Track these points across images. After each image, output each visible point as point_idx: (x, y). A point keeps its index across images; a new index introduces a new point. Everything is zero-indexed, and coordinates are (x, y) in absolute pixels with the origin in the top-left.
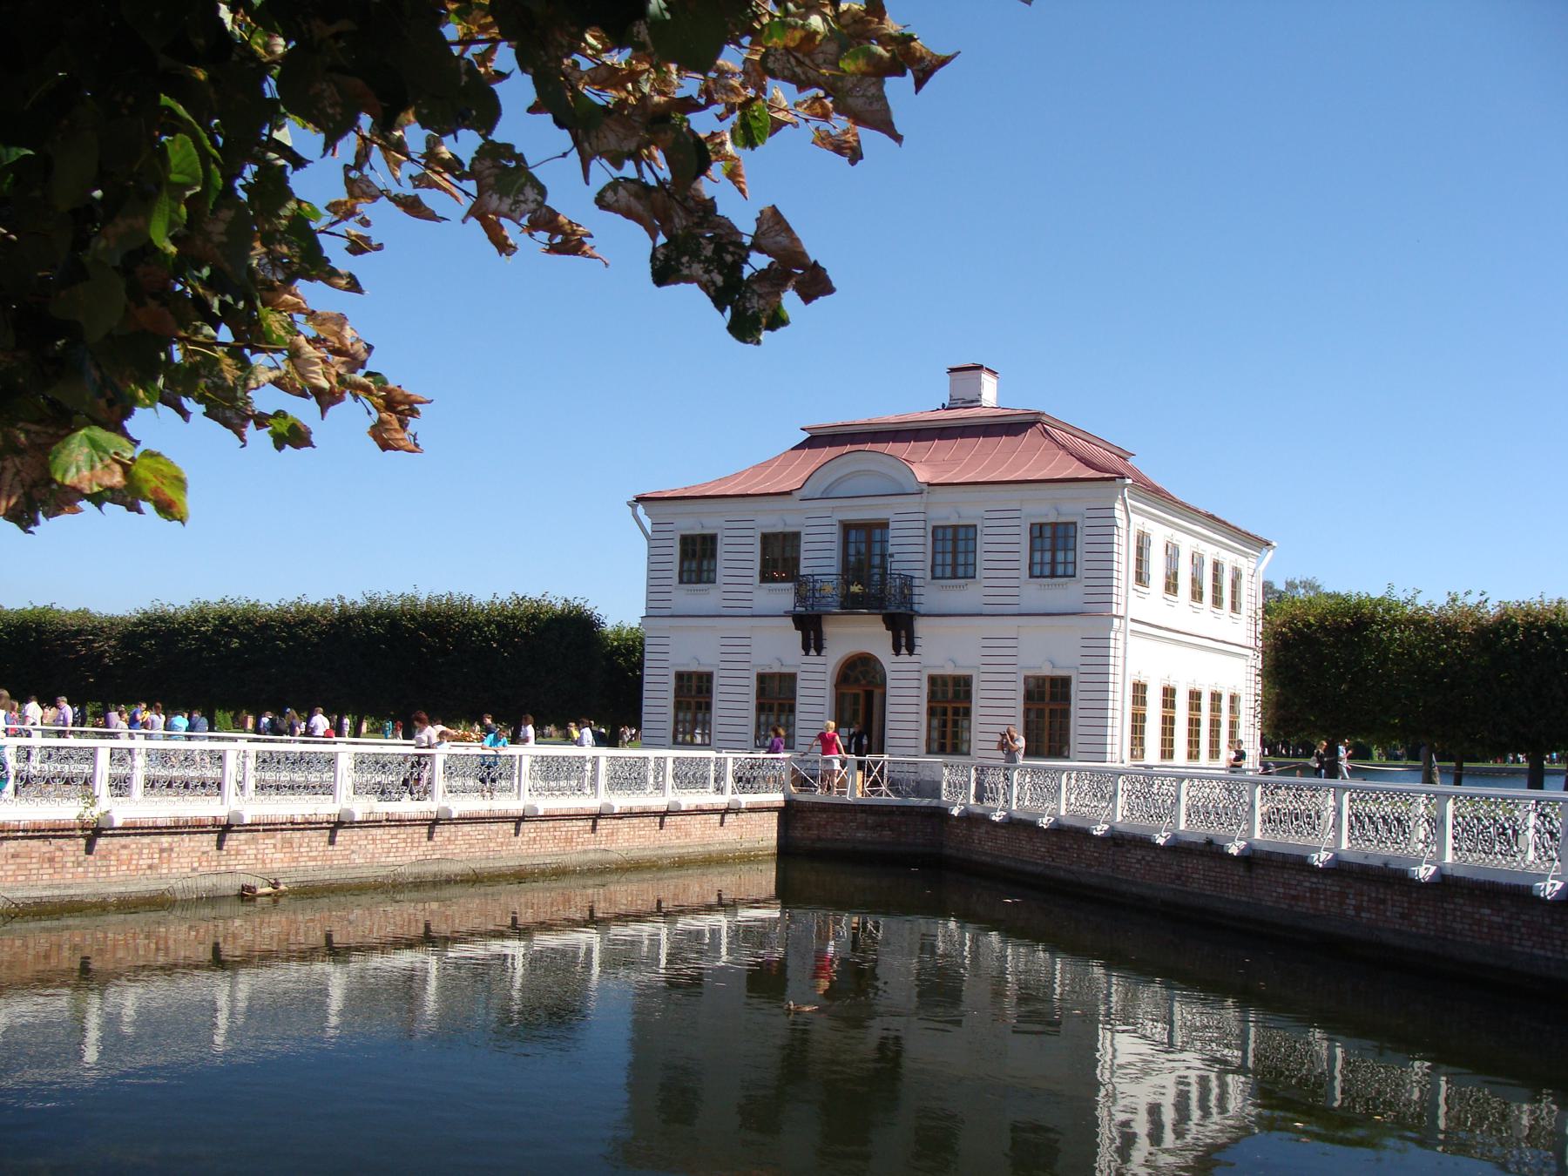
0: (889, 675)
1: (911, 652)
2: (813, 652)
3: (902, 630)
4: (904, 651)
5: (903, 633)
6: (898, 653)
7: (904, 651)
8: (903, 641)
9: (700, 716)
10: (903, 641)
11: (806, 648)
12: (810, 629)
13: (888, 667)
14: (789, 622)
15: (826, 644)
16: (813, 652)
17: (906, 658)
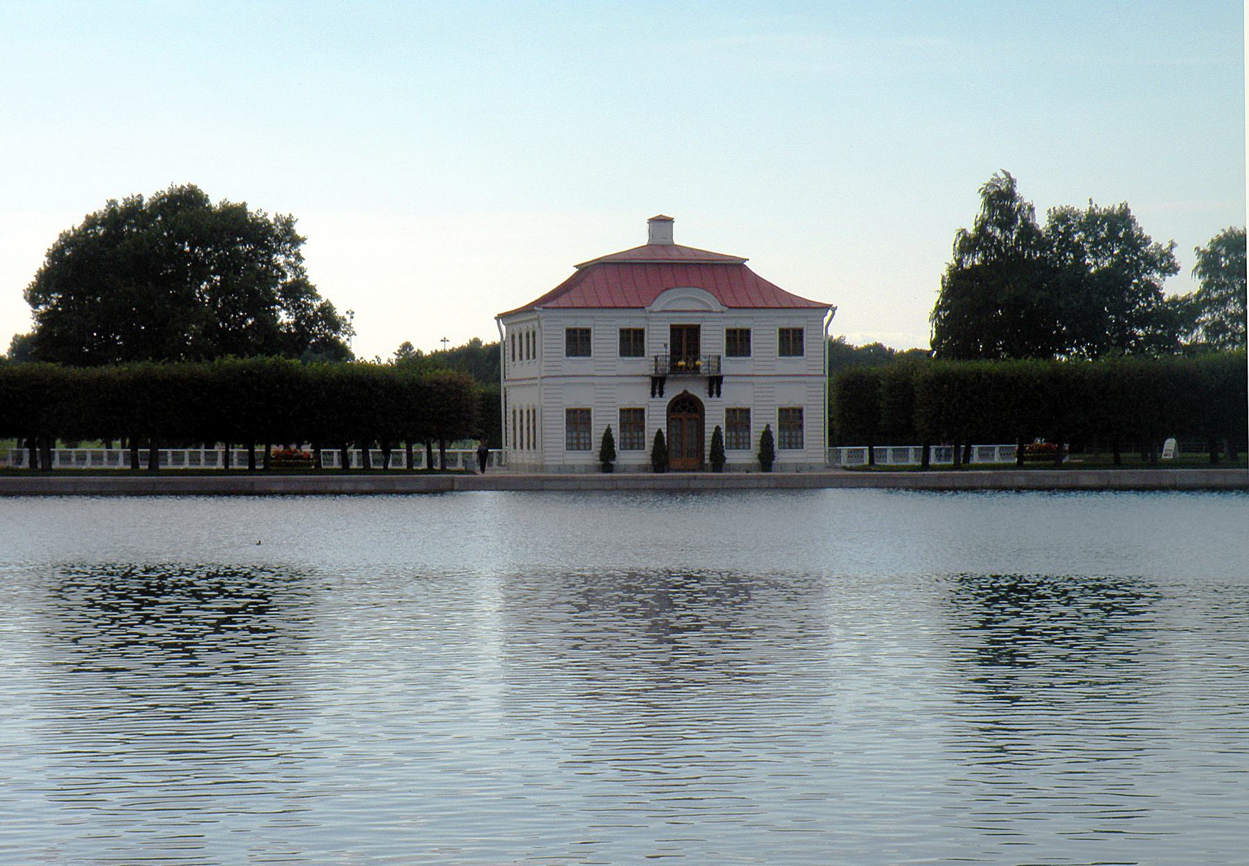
0: (706, 408)
1: (719, 394)
2: (657, 395)
3: (715, 384)
4: (715, 395)
5: (715, 386)
6: (711, 395)
7: (715, 395)
8: (715, 390)
9: (582, 435)
10: (715, 390)
11: (653, 394)
12: (658, 384)
13: (705, 404)
14: (648, 380)
15: (665, 391)
16: (657, 395)
17: (716, 399)
